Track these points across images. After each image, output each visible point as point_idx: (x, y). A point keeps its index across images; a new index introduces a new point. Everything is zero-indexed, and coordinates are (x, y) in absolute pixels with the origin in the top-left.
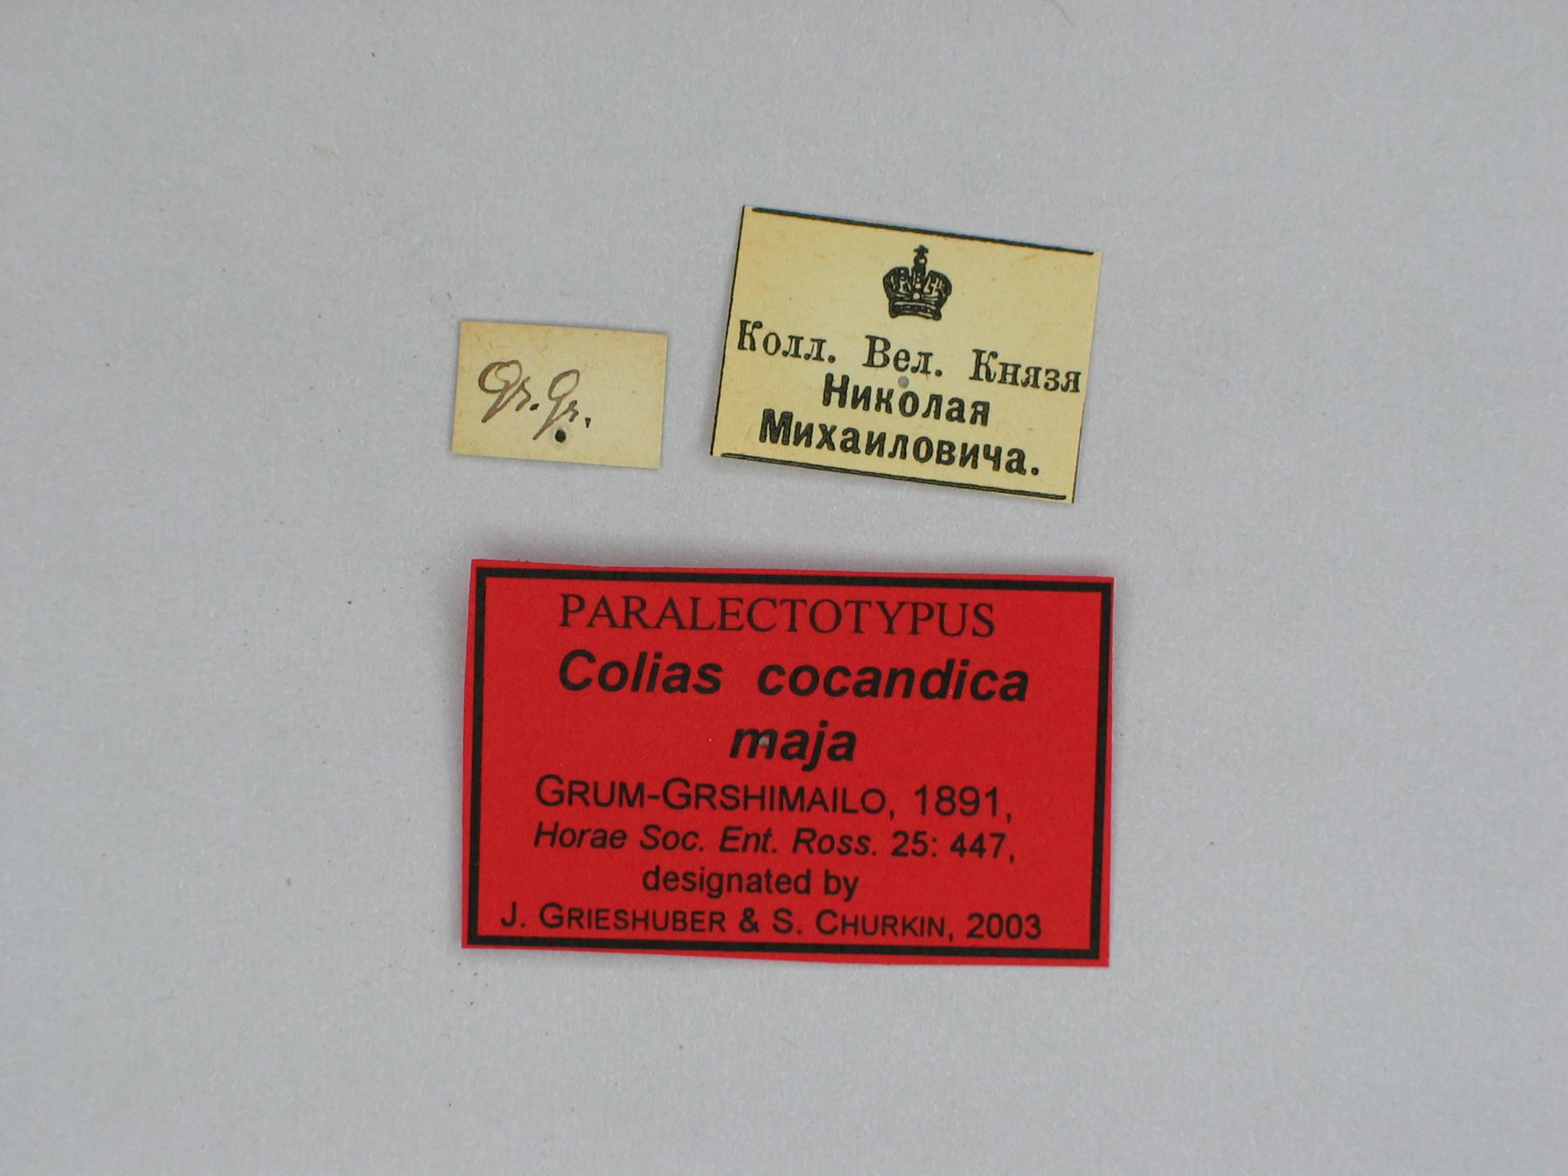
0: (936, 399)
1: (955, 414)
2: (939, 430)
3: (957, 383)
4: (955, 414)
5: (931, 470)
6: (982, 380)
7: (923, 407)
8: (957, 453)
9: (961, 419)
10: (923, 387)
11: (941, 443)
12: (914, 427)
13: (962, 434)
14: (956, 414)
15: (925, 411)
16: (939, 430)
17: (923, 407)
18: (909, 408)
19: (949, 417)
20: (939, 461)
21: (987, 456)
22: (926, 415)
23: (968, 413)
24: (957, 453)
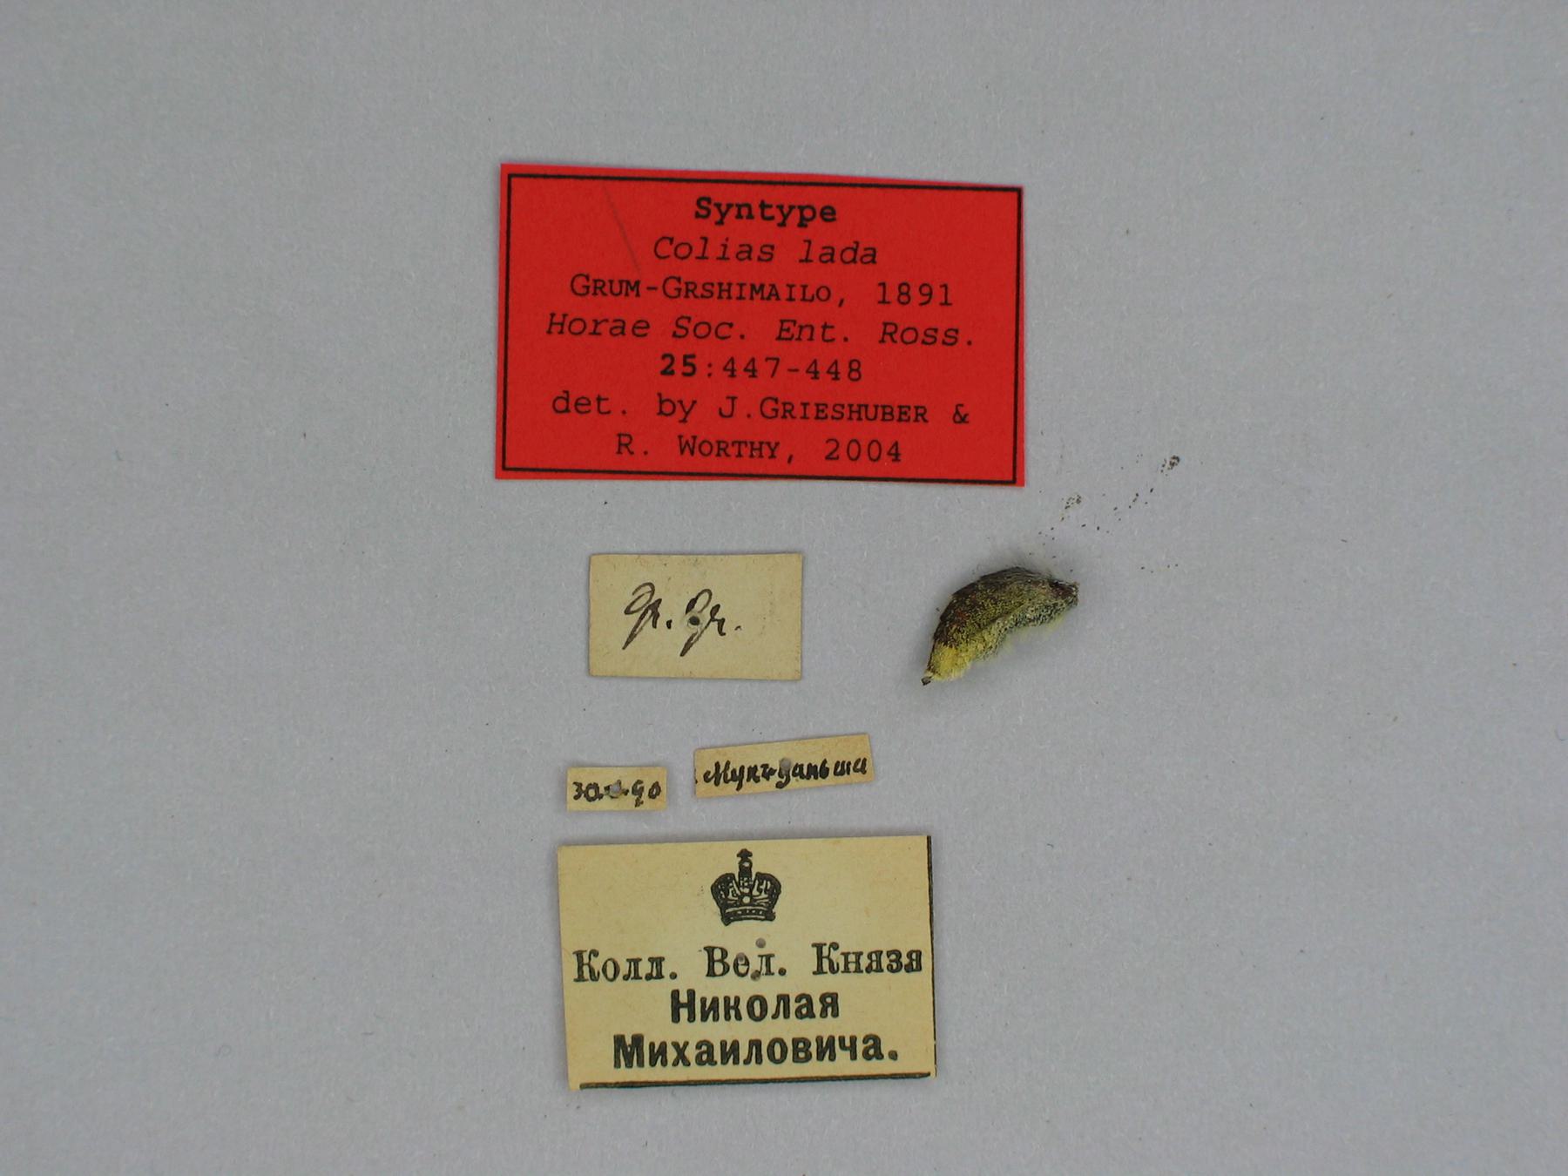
0: (783, 999)
1: (804, 1011)
2: (790, 1029)
3: (802, 979)
4: (804, 1011)
5: (789, 1069)
6: (826, 973)
7: (771, 1010)
8: (813, 1049)
9: (811, 1015)
10: (769, 988)
11: (795, 1042)
12: (768, 1030)
13: (813, 1029)
14: (806, 1010)
15: (774, 1012)
16: (790, 1029)
17: (771, 1010)
18: (757, 1011)
19: (799, 1015)
20: (796, 1059)
21: (843, 1047)
22: (775, 1016)
23: (817, 1007)
24: (813, 1049)
